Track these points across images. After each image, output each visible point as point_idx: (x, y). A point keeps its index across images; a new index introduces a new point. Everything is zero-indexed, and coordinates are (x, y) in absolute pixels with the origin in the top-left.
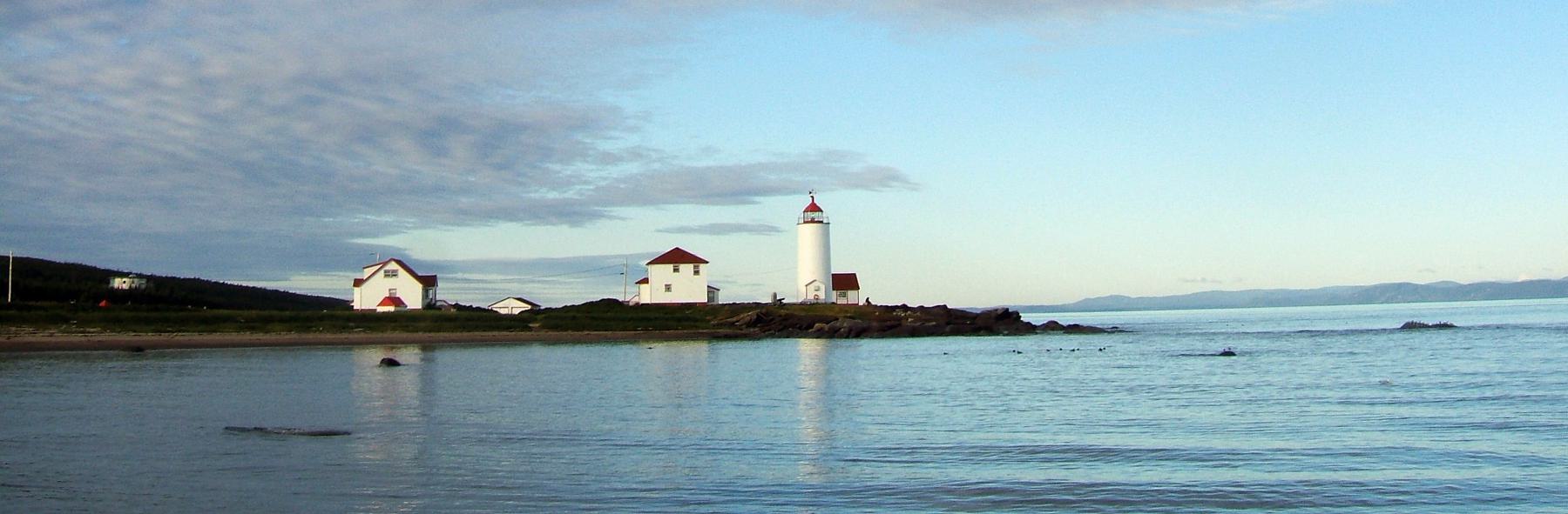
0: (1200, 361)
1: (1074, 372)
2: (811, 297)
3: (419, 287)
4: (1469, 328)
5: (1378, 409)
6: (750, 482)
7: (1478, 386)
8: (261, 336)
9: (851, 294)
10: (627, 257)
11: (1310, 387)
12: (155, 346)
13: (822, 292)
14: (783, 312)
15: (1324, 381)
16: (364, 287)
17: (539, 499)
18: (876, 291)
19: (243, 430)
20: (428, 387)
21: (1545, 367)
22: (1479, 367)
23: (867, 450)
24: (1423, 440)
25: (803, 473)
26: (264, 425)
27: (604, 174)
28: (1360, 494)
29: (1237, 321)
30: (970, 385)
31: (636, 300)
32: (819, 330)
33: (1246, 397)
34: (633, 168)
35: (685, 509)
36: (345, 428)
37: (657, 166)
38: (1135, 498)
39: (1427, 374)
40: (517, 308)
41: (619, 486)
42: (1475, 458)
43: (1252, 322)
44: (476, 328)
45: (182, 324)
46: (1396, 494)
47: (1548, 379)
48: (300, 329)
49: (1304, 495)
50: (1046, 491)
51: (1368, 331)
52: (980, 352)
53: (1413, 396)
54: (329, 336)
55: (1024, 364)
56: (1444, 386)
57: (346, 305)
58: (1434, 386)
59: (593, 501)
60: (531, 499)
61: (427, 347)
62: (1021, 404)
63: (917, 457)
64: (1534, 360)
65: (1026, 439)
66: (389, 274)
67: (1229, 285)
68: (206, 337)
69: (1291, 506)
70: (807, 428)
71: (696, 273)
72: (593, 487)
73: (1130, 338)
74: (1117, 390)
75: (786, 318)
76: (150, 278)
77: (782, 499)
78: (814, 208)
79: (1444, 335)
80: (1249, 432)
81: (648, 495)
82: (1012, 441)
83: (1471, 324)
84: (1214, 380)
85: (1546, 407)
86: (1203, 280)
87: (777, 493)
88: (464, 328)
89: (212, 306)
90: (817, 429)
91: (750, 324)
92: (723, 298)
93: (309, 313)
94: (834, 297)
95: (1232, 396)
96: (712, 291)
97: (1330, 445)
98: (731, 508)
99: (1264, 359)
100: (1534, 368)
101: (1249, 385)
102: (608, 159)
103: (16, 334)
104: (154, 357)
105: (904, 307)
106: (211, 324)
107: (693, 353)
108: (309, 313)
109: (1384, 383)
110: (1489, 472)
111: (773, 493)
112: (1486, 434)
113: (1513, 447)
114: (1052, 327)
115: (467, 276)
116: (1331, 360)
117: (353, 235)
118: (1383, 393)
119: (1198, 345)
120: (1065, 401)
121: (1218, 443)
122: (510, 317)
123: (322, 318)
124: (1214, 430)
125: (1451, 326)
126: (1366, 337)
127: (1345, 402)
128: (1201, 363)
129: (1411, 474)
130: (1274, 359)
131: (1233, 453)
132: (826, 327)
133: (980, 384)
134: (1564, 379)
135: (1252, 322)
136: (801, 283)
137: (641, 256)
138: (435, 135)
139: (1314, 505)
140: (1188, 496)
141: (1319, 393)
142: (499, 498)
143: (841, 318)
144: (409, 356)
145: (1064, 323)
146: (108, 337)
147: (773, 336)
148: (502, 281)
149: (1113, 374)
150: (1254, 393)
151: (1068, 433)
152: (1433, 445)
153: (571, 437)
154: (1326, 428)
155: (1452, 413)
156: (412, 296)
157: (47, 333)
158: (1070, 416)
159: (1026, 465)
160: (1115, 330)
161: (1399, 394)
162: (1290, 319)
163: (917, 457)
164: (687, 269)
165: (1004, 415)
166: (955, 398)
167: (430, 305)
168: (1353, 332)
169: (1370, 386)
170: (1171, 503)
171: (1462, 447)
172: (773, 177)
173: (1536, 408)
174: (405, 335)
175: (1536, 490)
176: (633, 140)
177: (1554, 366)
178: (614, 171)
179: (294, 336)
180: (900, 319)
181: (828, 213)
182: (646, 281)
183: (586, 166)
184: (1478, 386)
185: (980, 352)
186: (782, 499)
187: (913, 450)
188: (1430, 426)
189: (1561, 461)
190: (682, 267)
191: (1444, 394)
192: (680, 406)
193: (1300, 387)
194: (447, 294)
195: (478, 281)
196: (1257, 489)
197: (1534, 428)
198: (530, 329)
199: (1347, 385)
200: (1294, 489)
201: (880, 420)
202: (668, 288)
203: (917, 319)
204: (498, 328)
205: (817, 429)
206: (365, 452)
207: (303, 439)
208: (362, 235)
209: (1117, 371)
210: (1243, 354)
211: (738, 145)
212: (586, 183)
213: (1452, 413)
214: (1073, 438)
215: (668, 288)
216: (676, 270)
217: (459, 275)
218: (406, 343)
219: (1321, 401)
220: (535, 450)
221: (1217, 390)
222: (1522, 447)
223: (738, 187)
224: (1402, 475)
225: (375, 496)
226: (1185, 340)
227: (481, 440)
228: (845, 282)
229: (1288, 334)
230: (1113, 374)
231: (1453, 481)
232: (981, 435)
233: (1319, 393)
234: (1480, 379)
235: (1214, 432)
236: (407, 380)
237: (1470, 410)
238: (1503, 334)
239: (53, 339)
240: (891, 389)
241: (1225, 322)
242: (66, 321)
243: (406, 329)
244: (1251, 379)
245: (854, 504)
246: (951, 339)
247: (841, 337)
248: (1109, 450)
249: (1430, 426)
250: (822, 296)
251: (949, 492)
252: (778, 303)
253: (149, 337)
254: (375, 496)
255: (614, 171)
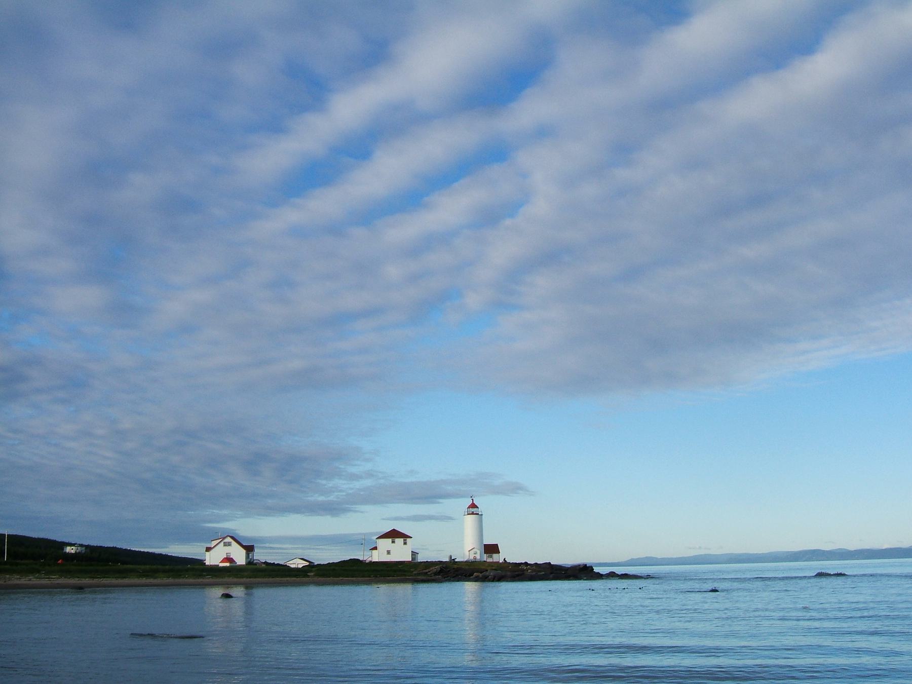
0: (698, 595)
1: (625, 601)
2: (472, 558)
3: (244, 552)
4: (855, 576)
5: (802, 623)
6: (436, 665)
7: (859, 609)
8: (151, 581)
9: (495, 556)
10: (364, 534)
11: (762, 610)
12: (90, 586)
13: (478, 555)
14: (455, 566)
15: (771, 607)
16: (212, 551)
17: (313, 675)
18: (510, 554)
19: (141, 635)
20: (249, 610)
21: (899, 598)
22: (861, 598)
23: (504, 647)
24: (828, 641)
25: (467, 660)
26: (154, 632)
27: (351, 486)
28: (791, 673)
29: (718, 571)
30: (564, 609)
31: (370, 559)
32: (476, 577)
33: (724, 616)
34: (368, 482)
35: (398, 681)
36: (201, 634)
37: (382, 481)
38: (660, 675)
39: (830, 603)
40: (301, 564)
41: (360, 668)
42: (858, 651)
43: (728, 572)
44: (277, 576)
45: (105, 574)
46: (812, 673)
47: (901, 606)
48: (174, 577)
49: (759, 673)
50: (608, 671)
51: (796, 578)
52: (570, 590)
53: (822, 615)
54: (191, 580)
55: (595, 597)
56: (840, 609)
57: (201, 562)
58: (834, 609)
59: (346, 677)
60: (309, 675)
61: (248, 587)
62: (594, 620)
63: (533, 651)
64: (892, 595)
65: (597, 640)
66: (226, 544)
67: (715, 551)
68: (120, 581)
69: (750, 679)
70: (469, 634)
71: (405, 543)
72: (345, 668)
73: (657, 581)
74: (650, 612)
75: (457, 570)
76: (87, 547)
77: (455, 675)
78: (473, 506)
79: (840, 580)
80: (726, 636)
81: (377, 673)
82: (589, 641)
83: (855, 573)
84: (706, 606)
85: (899, 622)
86: (700, 548)
87: (452, 672)
88: (270, 576)
89: (124, 563)
90: (475, 635)
91: (436, 574)
92: (421, 558)
93: (180, 567)
94: (485, 557)
95: (717, 615)
96: (414, 554)
97: (774, 644)
98: (426, 681)
99: (735, 594)
100: (892, 599)
101: (727, 609)
102: (354, 477)
103: (10, 579)
104: (91, 592)
105: (526, 564)
106: (123, 574)
107: (403, 590)
108: (180, 567)
109: (805, 608)
110: (866, 660)
111: (450, 672)
112: (864, 637)
113: (880, 645)
114: (612, 575)
115: (271, 545)
116: (774, 595)
117: (205, 522)
118: (805, 614)
119: (697, 586)
120: (619, 618)
121: (708, 643)
122: (297, 570)
123: (187, 570)
124: (706, 635)
125: (844, 575)
126: (794, 581)
127: (782, 619)
128: (698, 597)
129: (821, 661)
130: (741, 594)
131: (717, 648)
132: (481, 575)
133: (569, 609)
134: (910, 605)
135: (759, 673)
136: (466, 549)
137: (372, 534)
138: (253, 463)
139: (764, 679)
140: (691, 673)
141: (767, 613)
142: (290, 675)
143: (489, 570)
144: (238, 592)
145: (619, 573)
146: (63, 581)
147: (449, 581)
148: (292, 548)
149: (647, 602)
150: (729, 614)
151: (621, 637)
152: (833, 644)
153: (332, 640)
154: (771, 634)
155: (845, 625)
156: (240, 557)
157: (27, 578)
158: (622, 627)
159: (597, 655)
160: (648, 577)
161: (814, 614)
162: (750, 570)
163: (533, 651)
164: (400, 541)
165: (584, 626)
166: (556, 616)
167: (250, 563)
168: (787, 578)
169: (796, 609)
170: (681, 678)
171: (850, 645)
172: (450, 488)
173: (894, 622)
174: (235, 580)
175: (893, 670)
176: (368, 466)
177: (904, 598)
178: (357, 485)
179: (171, 580)
180: (524, 570)
181: (482, 509)
182: (375, 548)
183: (341, 481)
184: (859, 609)
185: (570, 590)
186: (455, 675)
187: (531, 647)
188: (832, 633)
189: (908, 653)
190: (397, 540)
191: (840, 614)
192: (395, 621)
193: (756, 610)
194: (260, 556)
195: (278, 548)
196: (731, 669)
197: (892, 634)
198: (308, 576)
199: (783, 609)
200: (753, 670)
201: (511, 629)
202: (389, 552)
203: (533, 571)
204: (290, 576)
205: (475, 635)
206: (213, 648)
207: (176, 640)
208: (210, 522)
209: (650, 601)
210: (723, 591)
211: (428, 470)
212: (341, 491)
213: (845, 625)
214: (623, 640)
215: (389, 552)
216: (393, 542)
217: (267, 545)
218: (237, 584)
219: (768, 618)
220: (311, 647)
221: (708, 612)
222: (886, 645)
223: (429, 493)
224: (816, 661)
225: (218, 674)
226: (690, 583)
227: (280, 641)
228: (492, 549)
229: (749, 579)
230: (647, 602)
231: (845, 665)
232: (571, 638)
233: (767, 613)
234: (861, 606)
235: (706, 637)
236: (237, 606)
237: (856, 623)
238: (874, 579)
239: (31, 582)
240: (518, 611)
241: (713, 572)
242: (39, 571)
243: (236, 576)
244: (728, 605)
245: (497, 678)
246: (553, 582)
247: (489, 581)
248: (645, 647)
249: (832, 633)
250: (478, 557)
251: (552, 671)
252: (453, 561)
253: (86, 581)
254: (218, 674)
255: (357, 485)
